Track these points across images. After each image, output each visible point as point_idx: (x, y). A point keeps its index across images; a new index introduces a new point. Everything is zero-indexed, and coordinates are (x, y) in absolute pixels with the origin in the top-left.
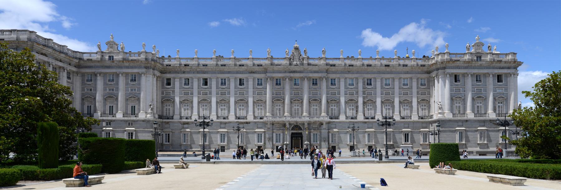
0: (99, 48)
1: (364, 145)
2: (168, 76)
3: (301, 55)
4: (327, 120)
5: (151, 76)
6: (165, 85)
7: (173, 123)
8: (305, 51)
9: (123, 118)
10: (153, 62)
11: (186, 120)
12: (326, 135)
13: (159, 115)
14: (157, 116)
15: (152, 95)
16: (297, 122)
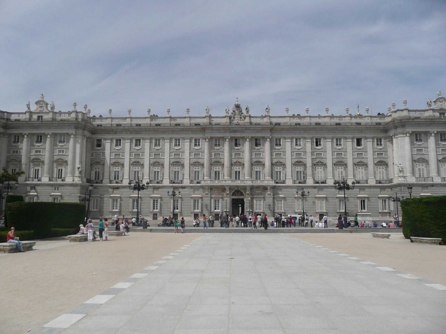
0: (28, 108)
1: (314, 213)
2: (99, 137)
3: (242, 114)
4: (271, 184)
5: (81, 137)
6: (95, 146)
7: (102, 187)
8: (247, 109)
9: (49, 182)
10: (84, 122)
11: (116, 185)
12: (271, 202)
13: (87, 179)
14: (85, 180)
15: (81, 158)
16: (237, 187)
